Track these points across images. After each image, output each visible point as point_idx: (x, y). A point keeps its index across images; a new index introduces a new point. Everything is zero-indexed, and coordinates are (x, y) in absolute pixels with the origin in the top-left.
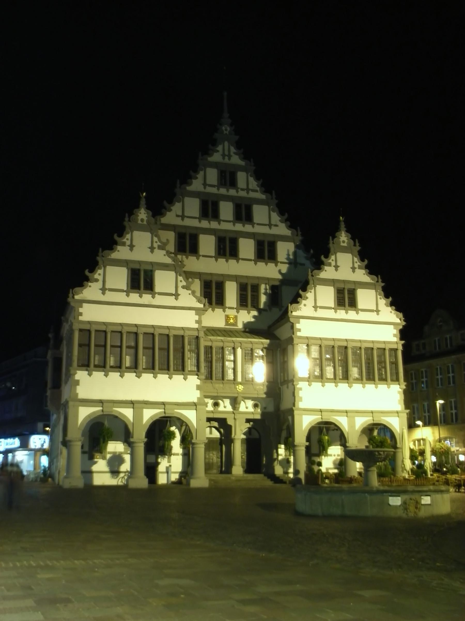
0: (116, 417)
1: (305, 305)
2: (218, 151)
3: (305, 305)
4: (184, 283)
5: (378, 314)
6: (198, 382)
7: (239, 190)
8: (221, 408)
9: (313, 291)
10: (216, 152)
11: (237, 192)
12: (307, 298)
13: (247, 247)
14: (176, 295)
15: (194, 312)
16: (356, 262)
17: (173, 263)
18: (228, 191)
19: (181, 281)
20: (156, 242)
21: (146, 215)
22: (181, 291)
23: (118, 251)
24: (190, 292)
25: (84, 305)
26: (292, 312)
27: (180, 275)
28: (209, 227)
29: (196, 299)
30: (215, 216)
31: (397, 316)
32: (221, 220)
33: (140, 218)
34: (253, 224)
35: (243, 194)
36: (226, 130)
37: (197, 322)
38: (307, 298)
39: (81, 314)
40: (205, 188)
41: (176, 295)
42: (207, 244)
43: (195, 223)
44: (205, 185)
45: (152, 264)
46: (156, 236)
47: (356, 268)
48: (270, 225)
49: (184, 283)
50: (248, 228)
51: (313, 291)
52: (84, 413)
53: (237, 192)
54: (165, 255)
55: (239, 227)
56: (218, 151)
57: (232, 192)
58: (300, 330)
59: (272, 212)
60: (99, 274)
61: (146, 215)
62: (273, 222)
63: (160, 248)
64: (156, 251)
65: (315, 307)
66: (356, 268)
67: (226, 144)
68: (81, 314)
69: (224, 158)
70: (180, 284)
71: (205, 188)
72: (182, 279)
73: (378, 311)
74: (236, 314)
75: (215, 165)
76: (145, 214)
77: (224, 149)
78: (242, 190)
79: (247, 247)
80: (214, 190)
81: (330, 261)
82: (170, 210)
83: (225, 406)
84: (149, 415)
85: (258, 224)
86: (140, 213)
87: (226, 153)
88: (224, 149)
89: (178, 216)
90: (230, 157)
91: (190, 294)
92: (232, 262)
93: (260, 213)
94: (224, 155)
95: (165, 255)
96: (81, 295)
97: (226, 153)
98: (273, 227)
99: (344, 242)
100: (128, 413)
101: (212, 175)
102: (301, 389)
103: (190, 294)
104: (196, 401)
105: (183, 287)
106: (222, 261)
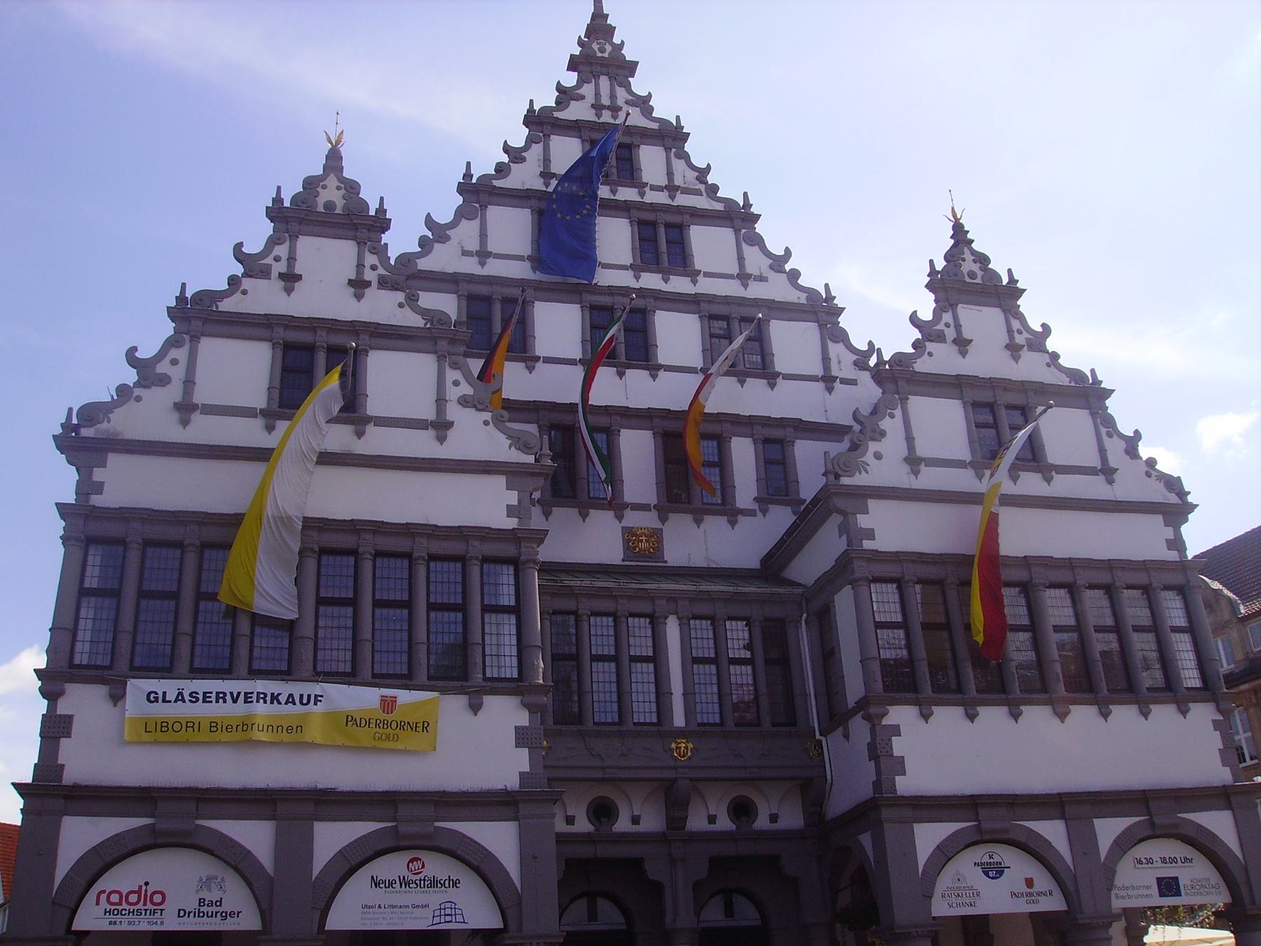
1: (878, 456)
2: (583, 98)
3: (878, 456)
5: (1110, 482)
6: (523, 718)
8: (623, 824)
9: (898, 412)
10: (577, 100)
11: (642, 194)
12: (883, 434)
14: (441, 427)
15: (501, 480)
16: (1020, 332)
19: (456, 383)
20: (374, 268)
21: (343, 191)
22: (454, 412)
23: (244, 292)
26: (837, 476)
27: (455, 366)
29: (509, 437)
34: (693, 275)
36: (602, 50)
37: (511, 512)
38: (883, 434)
39: (99, 488)
45: (355, 328)
46: (374, 251)
48: (744, 277)
50: (679, 285)
51: (898, 412)
54: (401, 305)
55: (651, 281)
56: (583, 98)
58: (870, 534)
59: (744, 246)
60: (174, 362)
61: (343, 191)
63: (383, 283)
64: (372, 293)
65: (914, 462)
67: (604, 82)
69: (599, 116)
70: (453, 393)
73: (1107, 472)
74: (658, 525)
75: (573, 128)
76: (338, 188)
77: (598, 95)
78: (653, 188)
79: (677, 336)
83: (639, 816)
85: (707, 275)
86: (324, 187)
87: (606, 101)
88: (598, 95)
89: (465, 253)
92: (636, 376)
93: (710, 246)
94: (598, 107)
95: (401, 305)
96: (105, 425)
97: (606, 101)
99: (972, 275)
102: (896, 730)
103: (486, 423)
104: (513, 783)
105: (464, 402)
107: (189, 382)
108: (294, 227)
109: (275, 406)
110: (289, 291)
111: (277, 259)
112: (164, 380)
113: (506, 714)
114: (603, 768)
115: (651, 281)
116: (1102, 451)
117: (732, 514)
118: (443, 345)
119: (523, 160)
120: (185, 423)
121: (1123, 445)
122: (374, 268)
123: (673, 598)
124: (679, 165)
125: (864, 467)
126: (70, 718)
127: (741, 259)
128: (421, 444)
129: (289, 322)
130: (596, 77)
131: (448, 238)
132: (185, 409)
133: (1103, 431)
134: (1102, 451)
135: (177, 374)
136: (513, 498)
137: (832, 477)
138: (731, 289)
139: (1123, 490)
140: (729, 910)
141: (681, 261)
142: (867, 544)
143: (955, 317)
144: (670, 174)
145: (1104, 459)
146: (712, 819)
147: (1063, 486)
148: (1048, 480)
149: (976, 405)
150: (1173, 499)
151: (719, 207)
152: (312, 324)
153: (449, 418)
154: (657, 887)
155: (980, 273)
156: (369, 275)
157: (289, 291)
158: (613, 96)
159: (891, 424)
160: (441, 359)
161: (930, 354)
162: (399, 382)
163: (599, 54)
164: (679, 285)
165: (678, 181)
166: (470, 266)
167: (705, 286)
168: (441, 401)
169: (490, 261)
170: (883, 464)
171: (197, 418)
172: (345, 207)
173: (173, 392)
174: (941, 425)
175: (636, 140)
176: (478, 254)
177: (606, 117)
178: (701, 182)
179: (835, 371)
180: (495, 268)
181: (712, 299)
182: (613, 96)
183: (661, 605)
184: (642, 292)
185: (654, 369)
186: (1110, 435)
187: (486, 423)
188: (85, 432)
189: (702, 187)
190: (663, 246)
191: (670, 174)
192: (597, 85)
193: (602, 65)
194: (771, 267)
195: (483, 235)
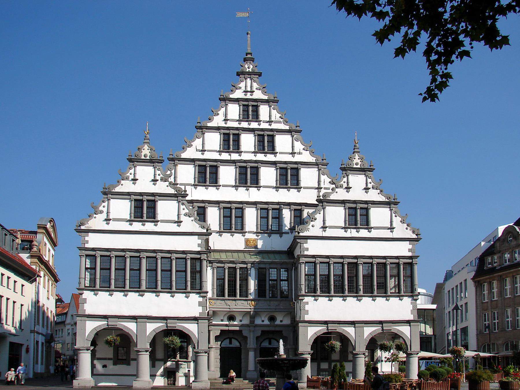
2: (240, 88)
4: (187, 211)
7: (262, 122)
9: (322, 212)
11: (259, 125)
13: (268, 175)
14: (179, 222)
17: (176, 193)
18: (249, 124)
19: (184, 209)
22: (183, 218)
26: (299, 233)
27: (183, 204)
31: (413, 232)
41: (179, 222)
42: (227, 174)
43: (216, 156)
44: (226, 120)
48: (293, 154)
49: (187, 211)
50: (270, 158)
52: (91, 326)
53: (259, 125)
55: (261, 157)
56: (240, 88)
57: (254, 125)
59: (295, 142)
67: (249, 81)
70: (183, 212)
71: (226, 123)
73: (391, 228)
75: (237, 101)
79: (268, 175)
80: (236, 125)
82: (190, 146)
85: (281, 153)
87: (249, 89)
90: (252, 92)
91: (192, 221)
93: (283, 142)
94: (246, 92)
97: (249, 89)
101: (234, 111)
103: (192, 221)
105: (186, 215)
115: (261, 157)
119: (218, 114)
121: (400, 219)
124: (274, 112)
125: (308, 230)
131: (192, 145)
133: (394, 215)
138: (288, 158)
139: (395, 235)
144: (270, 116)
145: (391, 224)
147: (374, 234)
150: (414, 236)
151: (287, 128)
153: (182, 220)
159: (319, 217)
160: (179, 202)
162: (166, 209)
164: (270, 158)
165: (273, 119)
167: (280, 158)
168: (179, 215)
169: (206, 152)
170: (314, 229)
174: (336, 215)
175: (259, 104)
176: (202, 151)
177: (249, 96)
178: (282, 118)
179: (322, 185)
180: (207, 156)
181: (281, 162)
184: (256, 162)
186: (396, 216)
189: (282, 120)
191: (270, 116)
193: (248, 75)
194: (304, 149)
195: (203, 144)
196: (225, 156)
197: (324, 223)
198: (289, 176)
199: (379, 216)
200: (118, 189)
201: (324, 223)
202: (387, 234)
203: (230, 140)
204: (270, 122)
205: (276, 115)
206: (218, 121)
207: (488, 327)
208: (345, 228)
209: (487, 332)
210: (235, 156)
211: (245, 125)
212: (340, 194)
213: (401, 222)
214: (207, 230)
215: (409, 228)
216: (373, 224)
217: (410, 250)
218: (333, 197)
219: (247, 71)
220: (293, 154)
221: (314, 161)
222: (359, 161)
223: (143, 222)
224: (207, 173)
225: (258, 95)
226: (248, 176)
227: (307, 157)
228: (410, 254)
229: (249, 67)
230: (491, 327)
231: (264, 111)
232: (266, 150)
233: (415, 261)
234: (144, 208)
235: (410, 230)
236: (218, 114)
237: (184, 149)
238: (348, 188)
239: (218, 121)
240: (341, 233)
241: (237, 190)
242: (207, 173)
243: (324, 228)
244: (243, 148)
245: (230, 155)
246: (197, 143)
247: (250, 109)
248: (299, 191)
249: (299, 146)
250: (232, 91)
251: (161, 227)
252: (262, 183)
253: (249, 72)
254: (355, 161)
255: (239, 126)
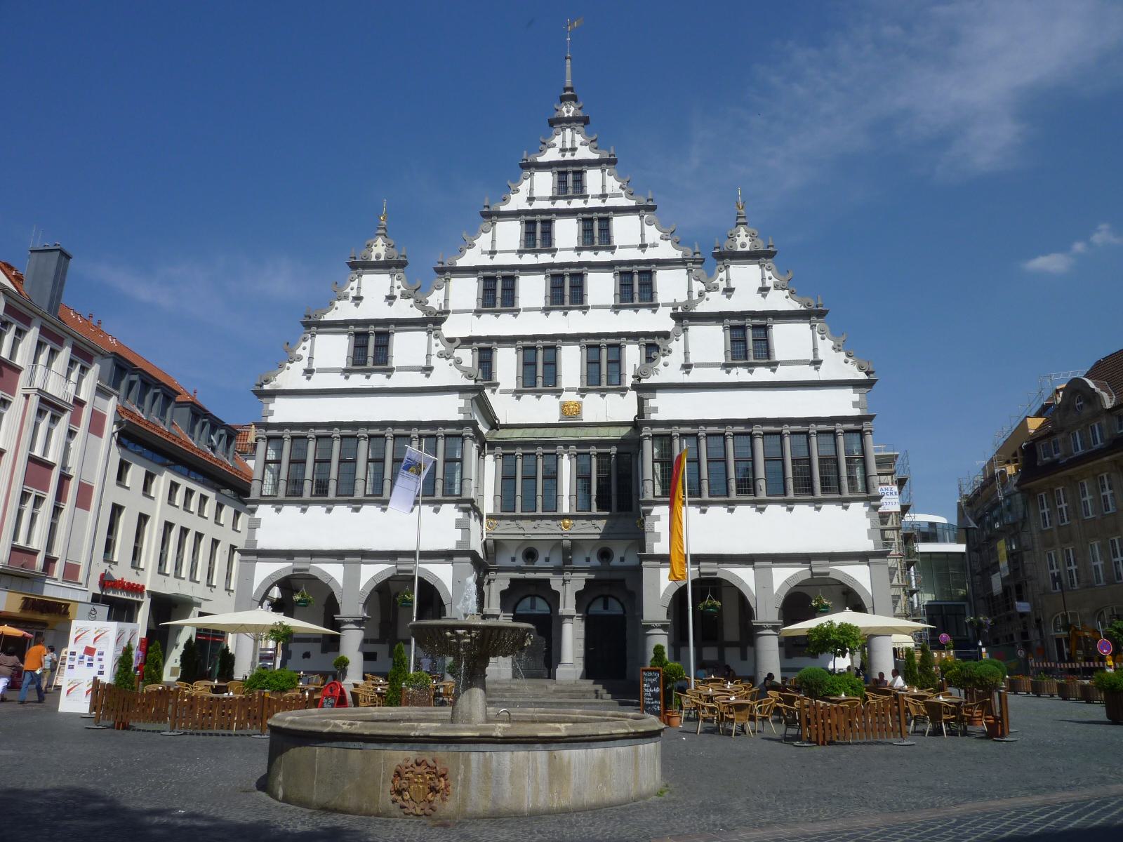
0: (316, 579)
1: (666, 365)
2: (554, 145)
5: (817, 369)
11: (586, 202)
13: (601, 287)
14: (427, 370)
18: (569, 203)
19: (437, 345)
22: (435, 361)
24: (451, 361)
25: (279, 400)
26: (639, 380)
27: (436, 337)
28: (536, 263)
30: (548, 244)
31: (860, 368)
32: (555, 250)
33: (374, 254)
35: (594, 203)
37: (461, 410)
38: (670, 352)
39: (271, 413)
40: (531, 205)
41: (427, 370)
42: (532, 290)
43: (513, 260)
44: (531, 199)
45: (387, 322)
47: (767, 289)
48: (643, 246)
49: (442, 348)
51: (682, 337)
53: (586, 202)
55: (588, 256)
56: (554, 145)
58: (655, 410)
62: (648, 241)
66: (767, 289)
67: (568, 130)
68: (271, 413)
69: (563, 156)
70: (435, 351)
72: (440, 343)
76: (383, 245)
77: (564, 142)
79: (601, 287)
80: (547, 205)
81: (717, 281)
82: (472, 246)
84: (370, 573)
85: (621, 247)
86: (376, 246)
88: (564, 142)
90: (573, 150)
92: (575, 314)
93: (625, 230)
94: (563, 150)
98: (648, 249)
99: (743, 245)
100: (334, 572)
101: (544, 183)
102: (658, 518)
105: (440, 355)
106: (556, 315)
107: (311, 358)
108: (360, 270)
109: (480, 308)
110: (357, 305)
111: (352, 289)
112: (300, 358)
113: (450, 512)
114: (524, 534)
115: (588, 256)
116: (815, 350)
117: (623, 391)
118: (431, 326)
119: (518, 191)
120: (309, 378)
121: (832, 343)
122: (399, 288)
123: (566, 444)
126: (259, 520)
127: (642, 235)
128: (419, 380)
129: (357, 323)
130: (563, 130)
131: (474, 245)
132: (309, 372)
134: (815, 350)
135: (305, 354)
136: (462, 403)
137: (636, 379)
138: (636, 255)
140: (606, 607)
141: (606, 242)
142: (653, 417)
143: (727, 275)
144: (604, 186)
145: (815, 355)
146: (588, 560)
147: (782, 374)
148: (774, 371)
149: (732, 328)
150: (862, 376)
151: (633, 203)
152: (367, 323)
154: (557, 594)
155: (748, 244)
156: (397, 293)
157: (357, 305)
158: (573, 141)
159: (676, 346)
161: (707, 299)
162: (407, 348)
163: (566, 115)
164: (604, 256)
165: (608, 191)
166: (486, 261)
167: (620, 255)
168: (428, 356)
170: (667, 370)
171: (315, 375)
172: (386, 256)
173: (304, 364)
174: (709, 343)
177: (568, 156)
178: (623, 189)
180: (500, 260)
181: (621, 263)
182: (573, 141)
183: (560, 448)
185: (585, 309)
187: (451, 365)
188: (266, 387)
189: (623, 192)
190: (596, 233)
192: (564, 136)
194: (661, 238)
195: (493, 241)
196: (529, 259)
197: (687, 358)
198: (636, 284)
199: (790, 340)
200: (329, 316)
201: (687, 358)
202: (809, 374)
203: (538, 229)
204: (604, 196)
205: (613, 184)
206: (517, 202)
207: (1057, 579)
208: (727, 366)
209: (1059, 590)
210: (544, 258)
211: (561, 204)
212: (715, 303)
213: (834, 348)
214: (476, 381)
215: (850, 360)
216: (778, 355)
217: (855, 405)
218: (701, 308)
219: (566, 116)
220: (643, 246)
221: (680, 257)
222: (747, 240)
223: (368, 372)
224: (498, 289)
225: (584, 153)
226: (567, 288)
227: (667, 250)
228: (856, 412)
229: (568, 110)
230: (1063, 578)
231: (593, 179)
232: (597, 244)
233: (866, 426)
234: (371, 345)
235: (853, 363)
236: (518, 191)
237: (461, 252)
238: (729, 291)
239: (517, 202)
240: (719, 376)
241: (547, 315)
242: (498, 289)
243: (687, 367)
244: (558, 243)
245: (536, 256)
246: (483, 241)
247: (570, 176)
248: (654, 312)
249: (653, 234)
250: (541, 151)
251: (399, 380)
252: (590, 300)
253: (569, 117)
254: (739, 241)
255: (552, 207)
